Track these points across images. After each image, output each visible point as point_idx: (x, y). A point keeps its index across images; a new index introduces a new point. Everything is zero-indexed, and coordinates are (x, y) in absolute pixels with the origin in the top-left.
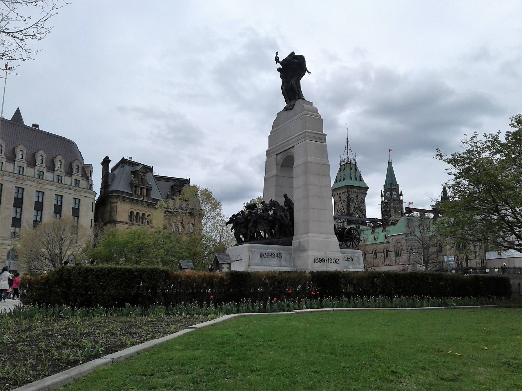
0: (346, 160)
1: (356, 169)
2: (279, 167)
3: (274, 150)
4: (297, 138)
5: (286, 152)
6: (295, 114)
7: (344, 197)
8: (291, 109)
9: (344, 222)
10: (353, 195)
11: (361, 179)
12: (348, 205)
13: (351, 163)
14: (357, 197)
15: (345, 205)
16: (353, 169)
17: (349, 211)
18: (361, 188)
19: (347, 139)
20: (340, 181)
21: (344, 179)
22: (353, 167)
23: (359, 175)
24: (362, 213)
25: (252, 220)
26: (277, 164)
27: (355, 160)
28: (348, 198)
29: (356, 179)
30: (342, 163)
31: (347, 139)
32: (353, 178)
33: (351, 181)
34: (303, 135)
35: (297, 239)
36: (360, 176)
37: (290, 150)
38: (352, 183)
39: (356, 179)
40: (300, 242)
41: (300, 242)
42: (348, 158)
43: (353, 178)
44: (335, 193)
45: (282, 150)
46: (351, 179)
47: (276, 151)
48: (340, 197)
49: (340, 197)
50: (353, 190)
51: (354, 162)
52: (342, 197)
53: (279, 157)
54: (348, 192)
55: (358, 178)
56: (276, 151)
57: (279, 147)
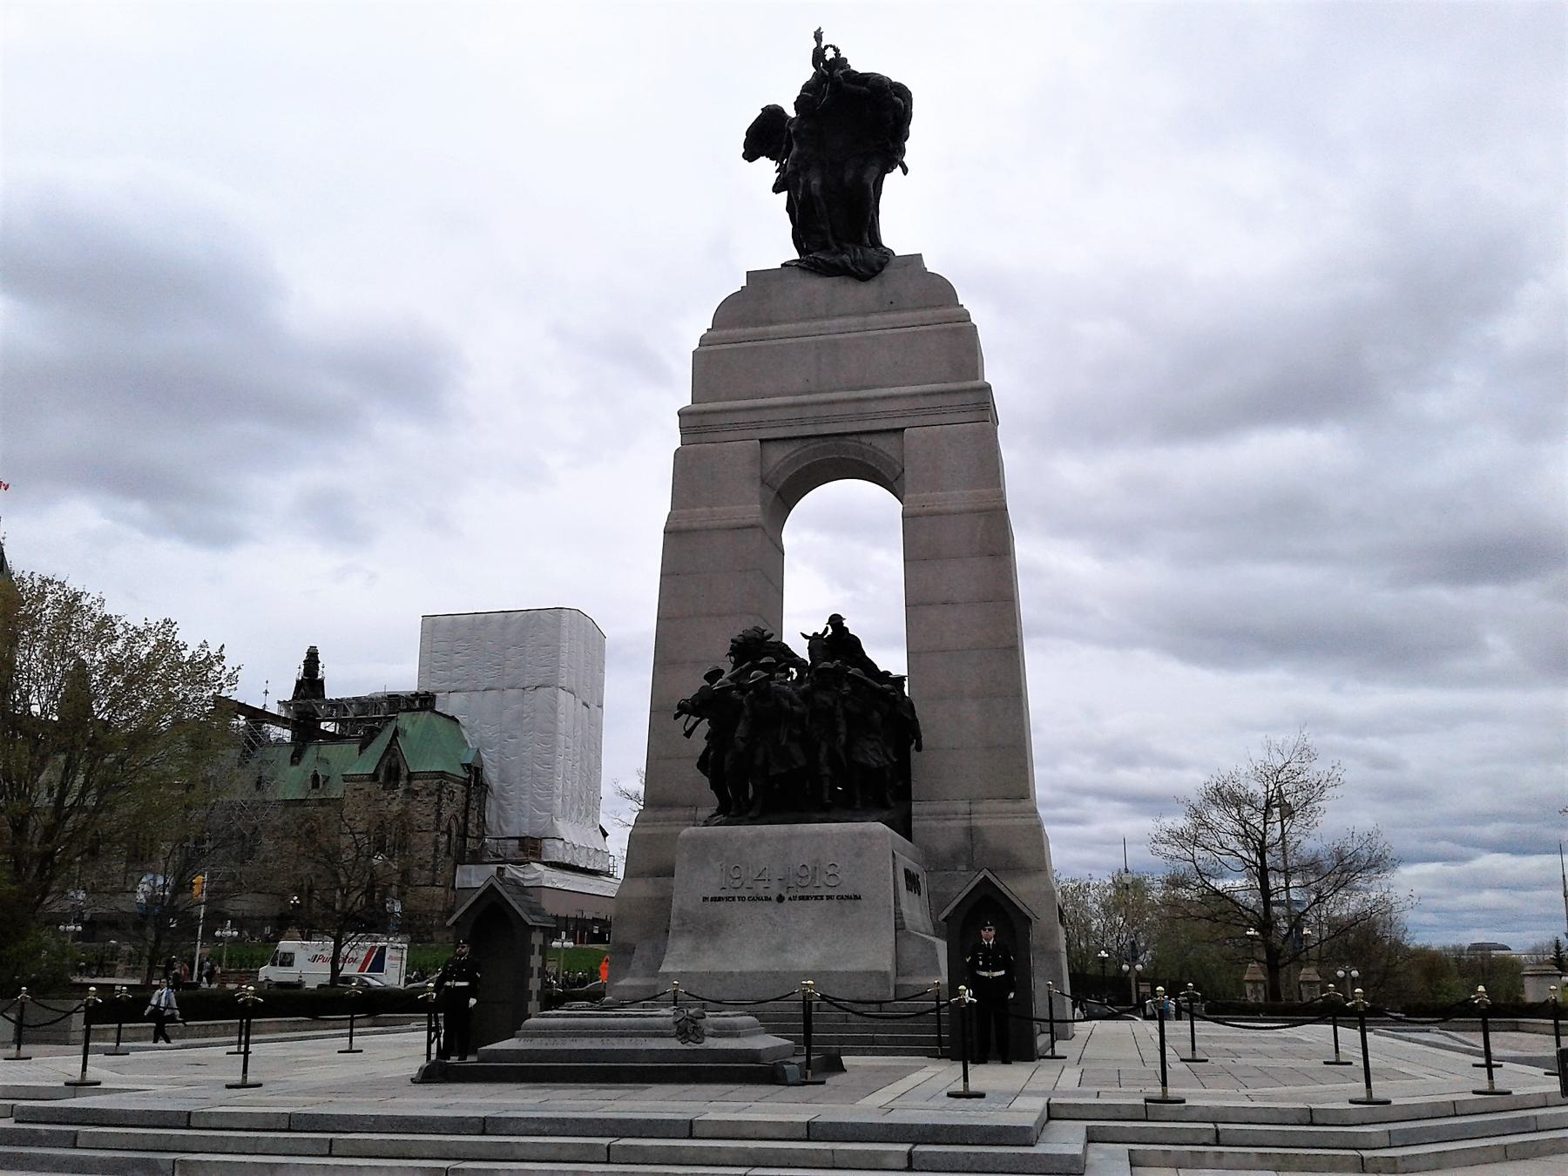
2: (773, 494)
3: (741, 417)
4: (923, 402)
5: (831, 442)
6: (893, 306)
8: (863, 278)
25: (840, 711)
26: (763, 482)
34: (971, 398)
35: (944, 815)
37: (864, 439)
40: (971, 832)
41: (971, 832)
47: (758, 425)
53: (777, 454)
56: (758, 425)
57: (778, 415)
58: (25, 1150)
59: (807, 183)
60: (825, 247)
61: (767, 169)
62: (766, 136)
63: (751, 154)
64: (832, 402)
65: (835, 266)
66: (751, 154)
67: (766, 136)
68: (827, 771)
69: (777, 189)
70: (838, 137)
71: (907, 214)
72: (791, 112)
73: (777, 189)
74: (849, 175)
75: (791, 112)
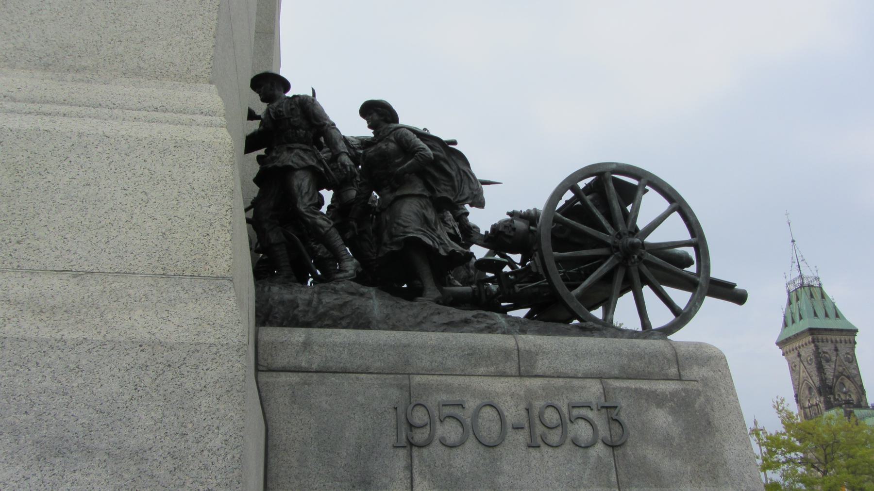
0: (798, 282)
1: (823, 296)
7: (808, 352)
9: (817, 405)
10: (827, 348)
11: (837, 315)
12: (820, 369)
13: (810, 286)
14: (836, 350)
15: (813, 369)
16: (818, 295)
17: (823, 380)
18: (841, 331)
19: (793, 241)
20: (793, 322)
21: (801, 318)
22: (818, 295)
23: (831, 306)
24: (854, 382)
27: (817, 279)
28: (817, 354)
29: (827, 315)
30: (792, 288)
31: (793, 241)
32: (821, 313)
33: (816, 320)
36: (835, 307)
38: (820, 323)
39: (827, 315)
42: (801, 276)
43: (821, 313)
44: (788, 348)
46: (816, 315)
48: (799, 355)
49: (799, 355)
50: (824, 337)
51: (816, 284)
52: (803, 354)
54: (813, 341)
55: (831, 313)
72: (289, 94)
75: (289, 94)
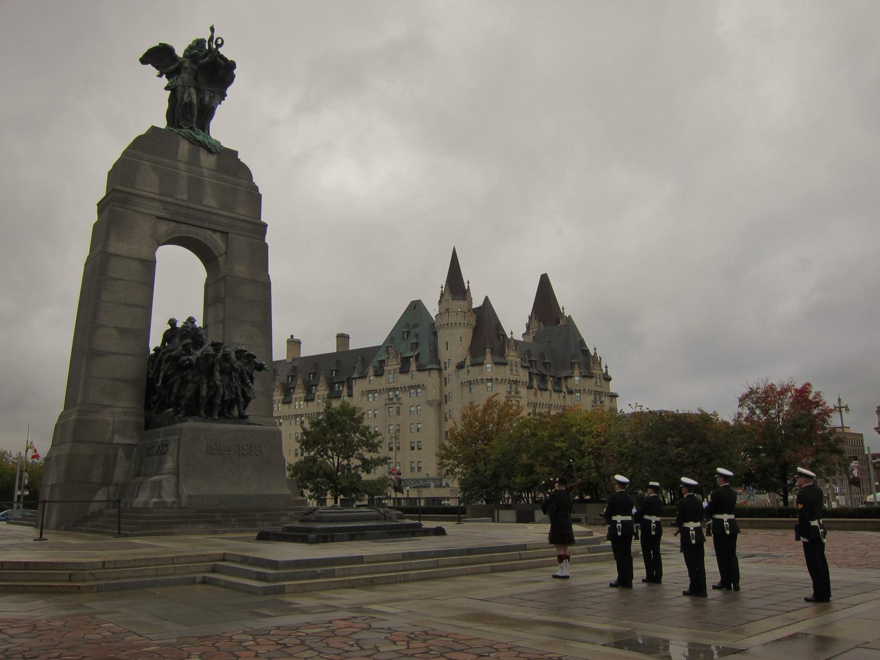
45: (181, 219)
58: (283, 583)
59: (190, 95)
60: (191, 128)
61: (151, 70)
62: (159, 57)
63: (144, 60)
64: (194, 209)
65: (199, 141)
66: (144, 60)
67: (159, 57)
68: (242, 400)
69: (167, 88)
70: (199, 76)
71: (224, 127)
72: (180, 53)
73: (167, 88)
74: (207, 98)
